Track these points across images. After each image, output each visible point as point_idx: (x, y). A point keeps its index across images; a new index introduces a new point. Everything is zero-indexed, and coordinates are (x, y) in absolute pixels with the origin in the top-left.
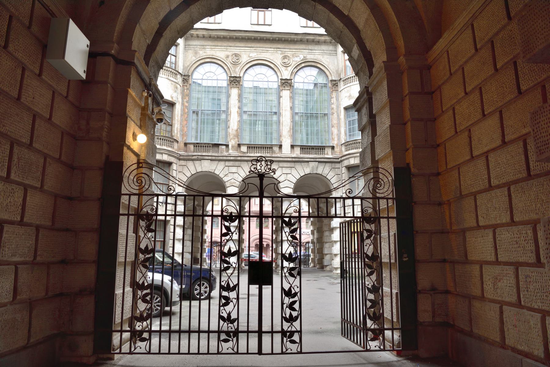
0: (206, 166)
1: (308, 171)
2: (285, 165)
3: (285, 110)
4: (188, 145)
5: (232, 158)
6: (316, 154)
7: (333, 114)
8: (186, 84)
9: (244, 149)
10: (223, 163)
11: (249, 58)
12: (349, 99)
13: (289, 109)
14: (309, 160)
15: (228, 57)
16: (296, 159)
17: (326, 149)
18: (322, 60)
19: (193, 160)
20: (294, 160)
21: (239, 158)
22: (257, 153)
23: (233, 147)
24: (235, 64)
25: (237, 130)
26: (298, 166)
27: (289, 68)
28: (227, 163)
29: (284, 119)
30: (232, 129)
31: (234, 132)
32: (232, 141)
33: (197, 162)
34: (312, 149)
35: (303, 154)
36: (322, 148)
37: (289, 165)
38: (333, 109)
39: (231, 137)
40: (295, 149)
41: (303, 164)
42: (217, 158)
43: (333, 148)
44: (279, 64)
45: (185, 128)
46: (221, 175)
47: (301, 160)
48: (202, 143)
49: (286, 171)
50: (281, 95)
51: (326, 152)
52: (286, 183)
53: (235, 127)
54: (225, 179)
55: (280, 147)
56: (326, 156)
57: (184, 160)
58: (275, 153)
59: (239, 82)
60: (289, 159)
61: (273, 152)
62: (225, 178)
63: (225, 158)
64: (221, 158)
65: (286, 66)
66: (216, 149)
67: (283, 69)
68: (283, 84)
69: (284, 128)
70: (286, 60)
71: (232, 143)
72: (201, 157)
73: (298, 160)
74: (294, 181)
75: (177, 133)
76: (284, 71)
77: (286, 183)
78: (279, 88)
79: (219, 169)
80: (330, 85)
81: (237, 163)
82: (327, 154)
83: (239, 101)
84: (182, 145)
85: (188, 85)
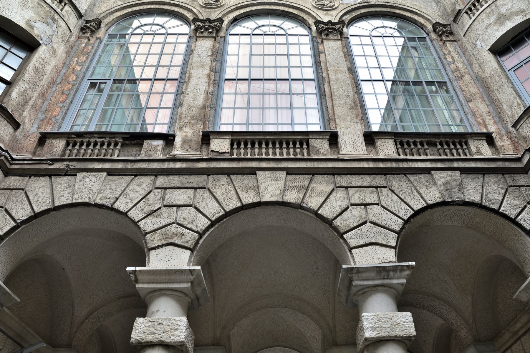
0: (90, 187)
1: (433, 195)
2: (355, 180)
5: (178, 165)
9: (220, 145)
10: (146, 182)
12: (502, 24)
14: (428, 165)
16: (389, 165)
20: (381, 165)
23: (185, 141)
26: (397, 183)
28: (161, 181)
29: (333, 86)
32: (186, 129)
34: (430, 144)
37: (367, 180)
38: (457, 69)
41: (412, 177)
42: (129, 166)
45: (57, 110)
46: (135, 214)
47: (405, 165)
48: (91, 134)
49: (356, 196)
52: (369, 233)
54: (147, 225)
55: (333, 139)
57: (22, 174)
58: (317, 152)
60: (365, 165)
62: (149, 220)
63: (155, 165)
64: (144, 165)
66: (135, 150)
68: (320, 32)
73: (394, 165)
74: (396, 224)
75: (23, 105)
77: (369, 233)
79: (129, 195)
81: (194, 180)
84: (33, 140)
85: (92, 40)
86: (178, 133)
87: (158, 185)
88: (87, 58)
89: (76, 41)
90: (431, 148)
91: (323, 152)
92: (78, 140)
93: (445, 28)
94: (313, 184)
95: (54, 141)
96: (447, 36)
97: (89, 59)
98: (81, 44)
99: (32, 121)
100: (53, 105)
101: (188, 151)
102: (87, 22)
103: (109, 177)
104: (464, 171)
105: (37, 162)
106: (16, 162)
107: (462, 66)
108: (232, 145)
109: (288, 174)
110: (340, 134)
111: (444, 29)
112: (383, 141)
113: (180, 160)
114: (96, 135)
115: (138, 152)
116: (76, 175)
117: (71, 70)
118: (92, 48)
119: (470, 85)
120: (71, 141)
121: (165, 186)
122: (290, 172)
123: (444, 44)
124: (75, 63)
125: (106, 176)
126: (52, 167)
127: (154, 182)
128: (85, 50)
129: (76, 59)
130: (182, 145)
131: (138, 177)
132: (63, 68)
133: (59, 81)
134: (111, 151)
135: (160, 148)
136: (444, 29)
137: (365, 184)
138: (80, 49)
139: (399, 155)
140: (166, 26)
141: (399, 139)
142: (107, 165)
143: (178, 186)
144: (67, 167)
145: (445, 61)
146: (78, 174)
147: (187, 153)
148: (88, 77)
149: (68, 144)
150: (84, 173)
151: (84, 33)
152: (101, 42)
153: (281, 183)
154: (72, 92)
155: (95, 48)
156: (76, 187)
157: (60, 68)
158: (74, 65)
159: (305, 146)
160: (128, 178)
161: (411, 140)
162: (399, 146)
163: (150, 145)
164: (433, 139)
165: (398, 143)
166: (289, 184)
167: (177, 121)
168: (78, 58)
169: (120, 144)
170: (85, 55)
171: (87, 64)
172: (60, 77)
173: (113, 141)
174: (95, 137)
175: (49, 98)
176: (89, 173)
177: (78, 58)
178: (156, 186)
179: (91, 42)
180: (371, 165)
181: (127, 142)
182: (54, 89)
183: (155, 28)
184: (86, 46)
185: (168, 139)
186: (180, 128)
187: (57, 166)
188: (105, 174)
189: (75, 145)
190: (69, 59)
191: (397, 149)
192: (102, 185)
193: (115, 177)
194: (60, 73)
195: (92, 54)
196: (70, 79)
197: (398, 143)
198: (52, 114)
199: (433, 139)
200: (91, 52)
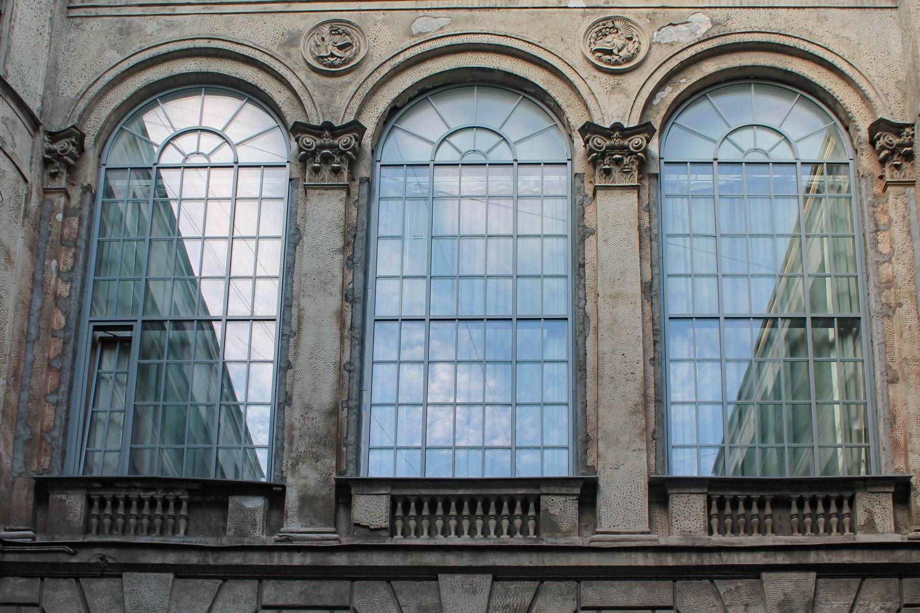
3: (615, 297)
4: (56, 497)
6: (802, 530)
7: (889, 311)
8: (62, 182)
9: (371, 510)
10: (245, 589)
11: (409, 42)
13: (638, 288)
15: (292, 40)
16: (685, 560)
17: (863, 501)
18: (818, 32)
19: (77, 573)
20: (669, 561)
21: (340, 560)
22: (445, 532)
23: (306, 500)
24: (330, 69)
25: (334, 412)
27: (633, 82)
29: (606, 346)
30: (308, 408)
31: (319, 424)
32: (304, 469)
33: (102, 585)
35: (722, 531)
36: (837, 492)
39: (301, 446)
40: (678, 502)
41: (723, 586)
43: (901, 490)
44: (576, 60)
47: (715, 560)
50: (589, 221)
51: (861, 517)
53: (325, 397)
56: (862, 537)
58: (554, 528)
59: (353, 158)
60: (640, 560)
61: (543, 523)
65: (615, 67)
66: (214, 516)
67: (596, 85)
68: (595, 159)
69: (606, 392)
70: (614, 41)
71: (307, 479)
72: (124, 557)
73: (694, 560)
76: (602, 98)
78: (575, 190)
80: (867, 162)
82: (870, 525)
83: (349, 263)
86: (290, 480)
87: (266, 601)
88: (75, 257)
89: (41, 205)
90: (779, 513)
91: (565, 526)
92: (108, 494)
93: (899, 135)
94: (539, 602)
95: (64, 497)
96: (897, 167)
97: (81, 262)
98: (53, 212)
99: (11, 447)
100: (39, 401)
101: (312, 524)
102: (54, 137)
103: (179, 581)
104: (825, 571)
105: (46, 548)
106: (11, 548)
107: (905, 270)
108: (393, 508)
109: (495, 579)
110: (602, 483)
111: (896, 141)
112: (685, 498)
113: (299, 549)
114: (138, 484)
115: (222, 523)
116: (121, 576)
117: (50, 299)
118: (80, 224)
119: (906, 335)
120: (95, 496)
121: (280, 602)
122: (499, 574)
123: (884, 190)
124: (55, 275)
125: (173, 581)
126: (74, 560)
127: (259, 595)
128: (66, 230)
129: (54, 262)
130: (301, 509)
131: (230, 583)
132: (32, 291)
133: (33, 331)
134: (171, 521)
135: (259, 516)
136: (896, 141)
137: (635, 602)
138: (56, 230)
139: (711, 532)
140: (233, 134)
141: (716, 495)
142: (171, 558)
143: (301, 603)
144: (102, 559)
145: (871, 252)
146: (124, 574)
147: (311, 529)
148: (87, 317)
149: (90, 503)
150: (135, 574)
151: (53, 176)
152: (94, 197)
153: (482, 598)
154: (67, 362)
155: (85, 223)
156: (127, 603)
157: (28, 294)
158: (53, 282)
159: (531, 513)
160: (211, 585)
161: (741, 495)
162: (714, 510)
163: (241, 509)
164: (786, 493)
165: (714, 503)
166: (496, 602)
167: (286, 445)
168: (57, 257)
169: (185, 504)
170: (69, 247)
171: (79, 277)
172: (33, 319)
173: (171, 496)
174: (136, 488)
175: (26, 380)
176: (143, 574)
177: (57, 257)
178: (263, 603)
179: (74, 202)
180: (650, 560)
181: (197, 499)
182: (30, 357)
183: (209, 142)
184: (65, 216)
185: (274, 494)
186: (294, 466)
187: (83, 557)
188: (171, 576)
189: (103, 503)
190: (39, 266)
191: (710, 517)
192: (170, 599)
193: (191, 583)
194: (30, 308)
195: (81, 243)
196: (55, 326)
197: (714, 503)
198: (42, 425)
199: (786, 493)
200: (78, 234)
